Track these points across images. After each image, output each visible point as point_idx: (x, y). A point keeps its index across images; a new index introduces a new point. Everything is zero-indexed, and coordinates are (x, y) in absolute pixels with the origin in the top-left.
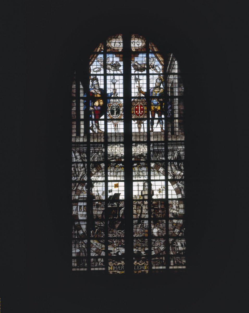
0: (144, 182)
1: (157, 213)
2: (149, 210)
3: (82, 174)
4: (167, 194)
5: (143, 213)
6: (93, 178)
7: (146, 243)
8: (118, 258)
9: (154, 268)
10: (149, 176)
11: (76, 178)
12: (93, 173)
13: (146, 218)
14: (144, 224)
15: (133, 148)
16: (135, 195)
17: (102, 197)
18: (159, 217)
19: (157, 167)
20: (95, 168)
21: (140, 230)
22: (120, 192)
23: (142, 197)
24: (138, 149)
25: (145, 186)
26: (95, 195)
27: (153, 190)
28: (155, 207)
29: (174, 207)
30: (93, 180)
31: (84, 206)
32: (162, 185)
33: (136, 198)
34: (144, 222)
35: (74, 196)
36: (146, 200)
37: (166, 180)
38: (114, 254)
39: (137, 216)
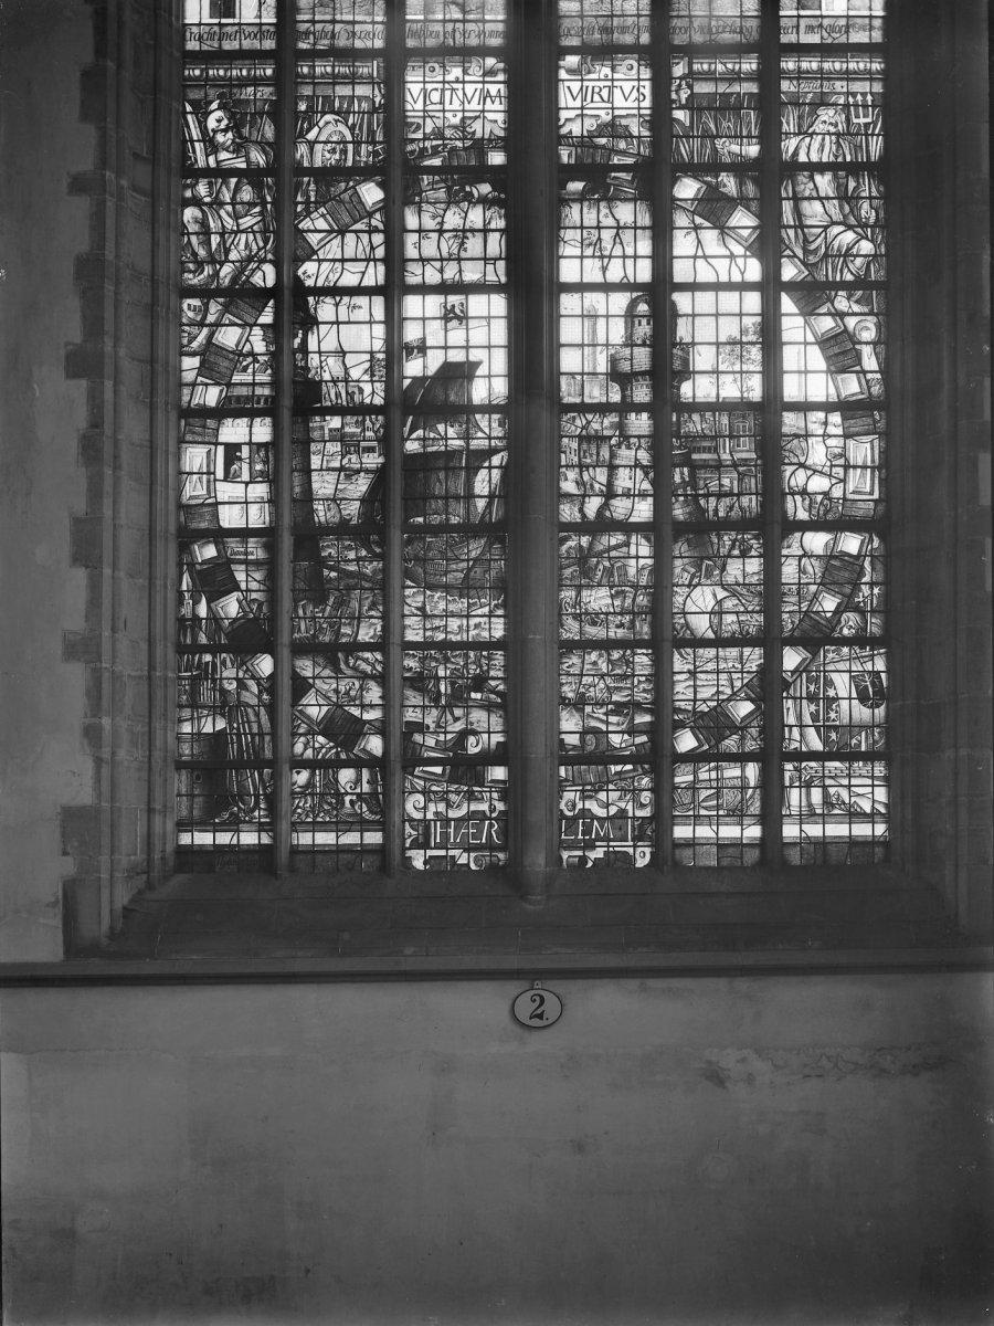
2: (658, 471)
3: (242, 246)
4: (772, 371)
6: (310, 272)
7: (639, 682)
8: (464, 769)
9: (681, 832)
10: (662, 257)
11: (208, 270)
12: (313, 239)
15: (567, 84)
17: (367, 388)
19: (714, 208)
20: (322, 210)
22: (475, 355)
24: (597, 90)
26: (327, 377)
28: (694, 456)
29: (817, 454)
30: (309, 283)
31: (250, 443)
35: (194, 385)
36: (639, 408)
37: (770, 287)
38: (439, 746)
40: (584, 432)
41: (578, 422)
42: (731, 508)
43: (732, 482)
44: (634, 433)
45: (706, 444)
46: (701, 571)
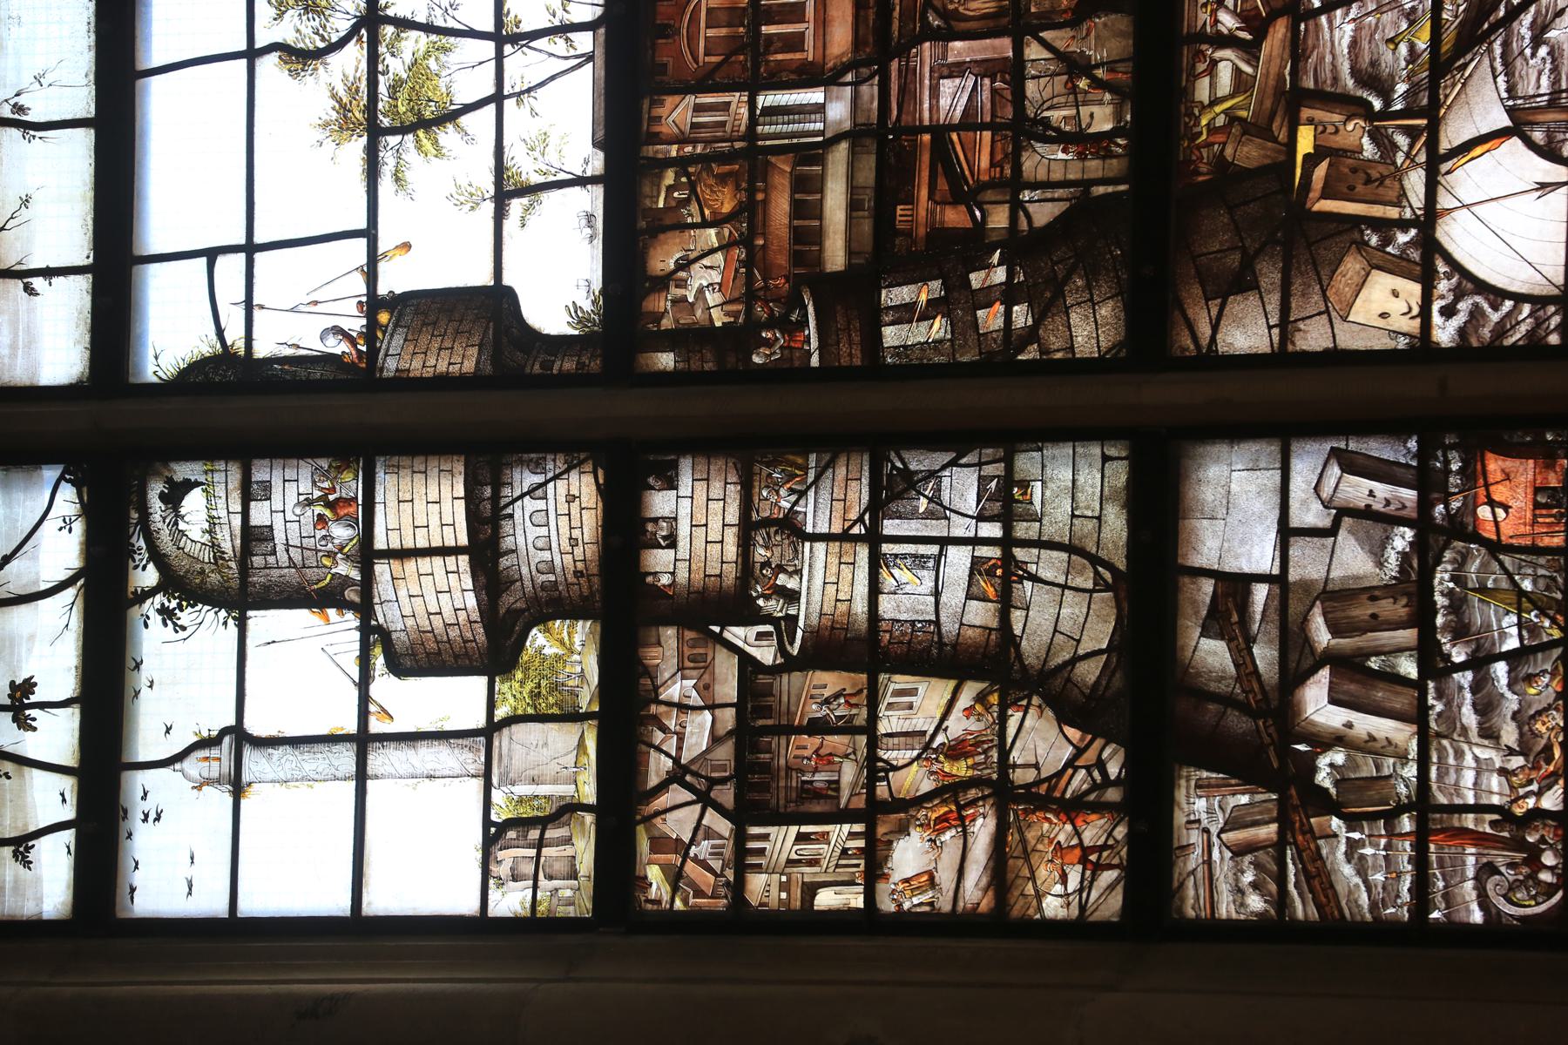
0: (149, 577)
1: (1012, 185)
5: (981, 614)
13: (1116, 523)
14: (1308, 564)
16: (494, 834)
18: (1101, 118)
21: (1487, 707)
23: (537, 639)
25: (253, 537)
27: (356, 324)
28: (835, 255)
32: (252, 54)
33: (568, 810)
34: (1235, 586)
39: (1073, 809)
40: (726, 795)
41: (679, 824)
42: (1073, 66)
43: (957, 70)
44: (731, 551)
45: (781, 207)
46: (1356, 221)
